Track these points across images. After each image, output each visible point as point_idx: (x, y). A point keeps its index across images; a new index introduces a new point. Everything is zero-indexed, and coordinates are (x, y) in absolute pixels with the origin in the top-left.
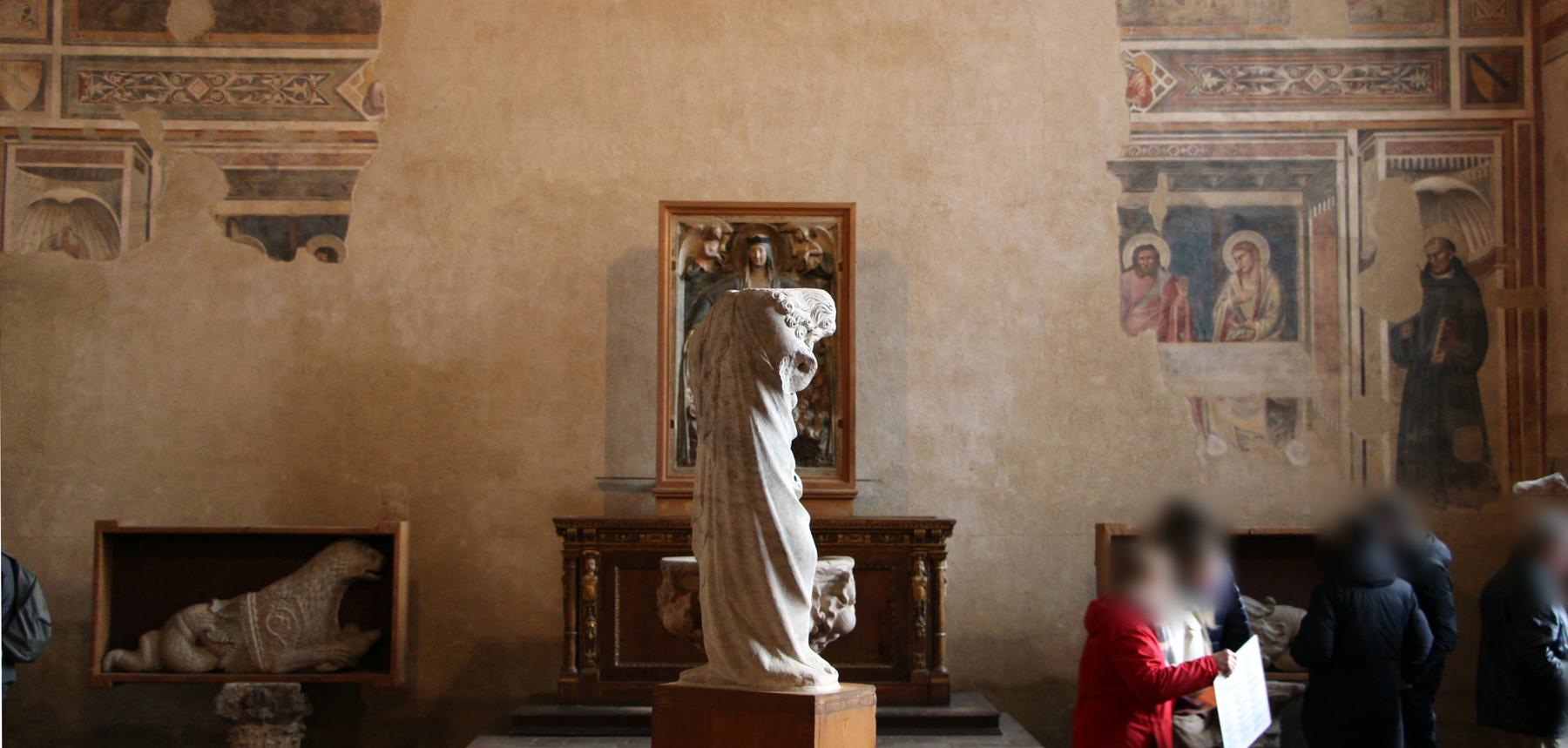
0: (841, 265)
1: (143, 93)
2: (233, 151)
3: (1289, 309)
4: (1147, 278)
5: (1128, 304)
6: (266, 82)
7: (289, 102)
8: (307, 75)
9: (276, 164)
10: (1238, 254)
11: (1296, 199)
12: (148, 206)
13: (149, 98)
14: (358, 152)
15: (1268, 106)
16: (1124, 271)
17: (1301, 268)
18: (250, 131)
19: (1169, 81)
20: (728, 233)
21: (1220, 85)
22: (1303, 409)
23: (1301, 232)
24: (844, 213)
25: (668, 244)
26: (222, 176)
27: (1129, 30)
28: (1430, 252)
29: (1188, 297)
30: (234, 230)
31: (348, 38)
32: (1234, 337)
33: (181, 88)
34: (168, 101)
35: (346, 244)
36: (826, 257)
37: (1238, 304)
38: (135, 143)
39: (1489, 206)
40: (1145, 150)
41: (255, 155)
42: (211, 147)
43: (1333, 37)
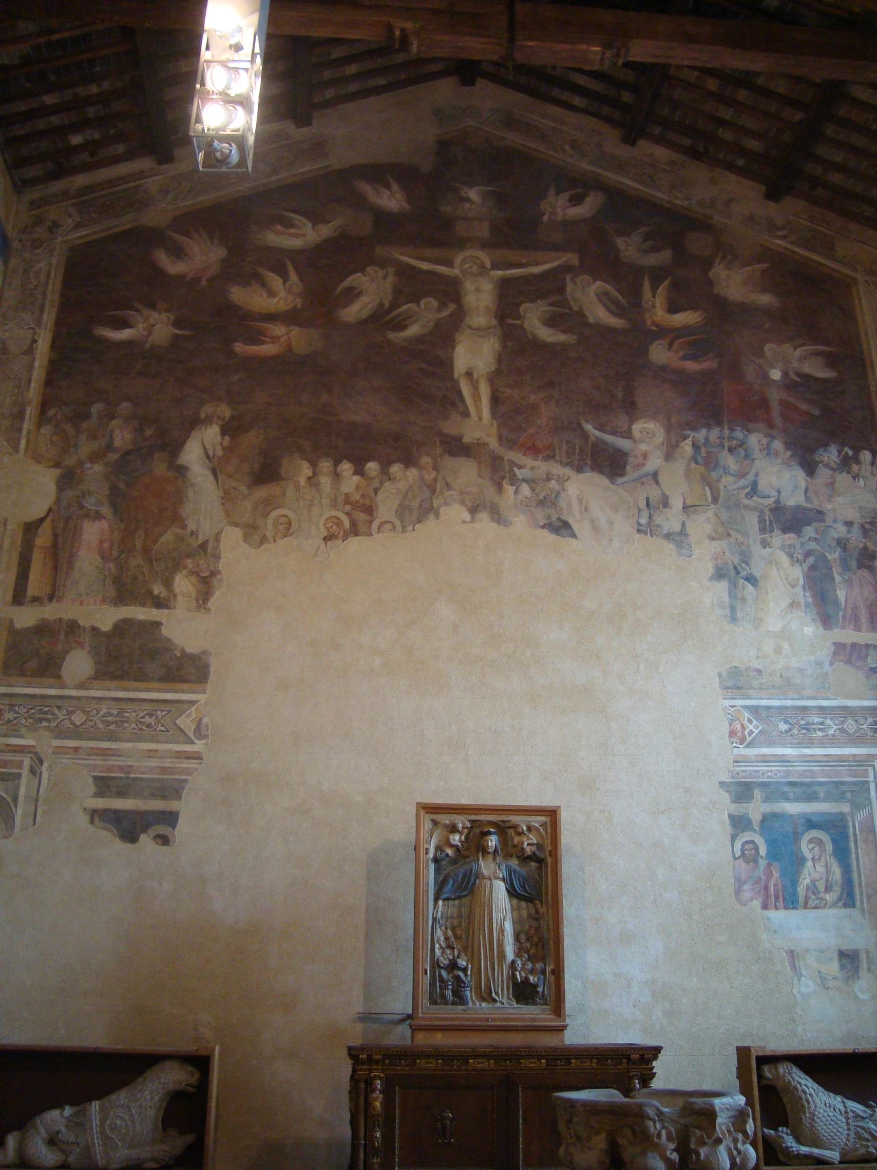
0: (550, 852)
1: (41, 720)
2: (99, 762)
3: (848, 884)
4: (752, 864)
5: (739, 883)
6: (126, 714)
7: (141, 729)
8: (156, 711)
9: (130, 773)
10: (811, 846)
11: (846, 808)
12: (37, 800)
13: (44, 724)
14: (188, 766)
15: (822, 745)
16: (735, 859)
17: (853, 856)
18: (113, 749)
19: (756, 727)
20: (466, 828)
21: (790, 730)
22: (863, 957)
23: (851, 831)
24: (552, 814)
25: (424, 834)
26: (90, 781)
27: (728, 692)
30: (96, 819)
31: (186, 686)
32: (813, 905)
33: (67, 717)
34: (57, 726)
35: (176, 832)
36: (539, 846)
37: (813, 882)
38: (32, 755)
40: (744, 774)
41: (114, 766)
42: (85, 759)
43: (858, 699)
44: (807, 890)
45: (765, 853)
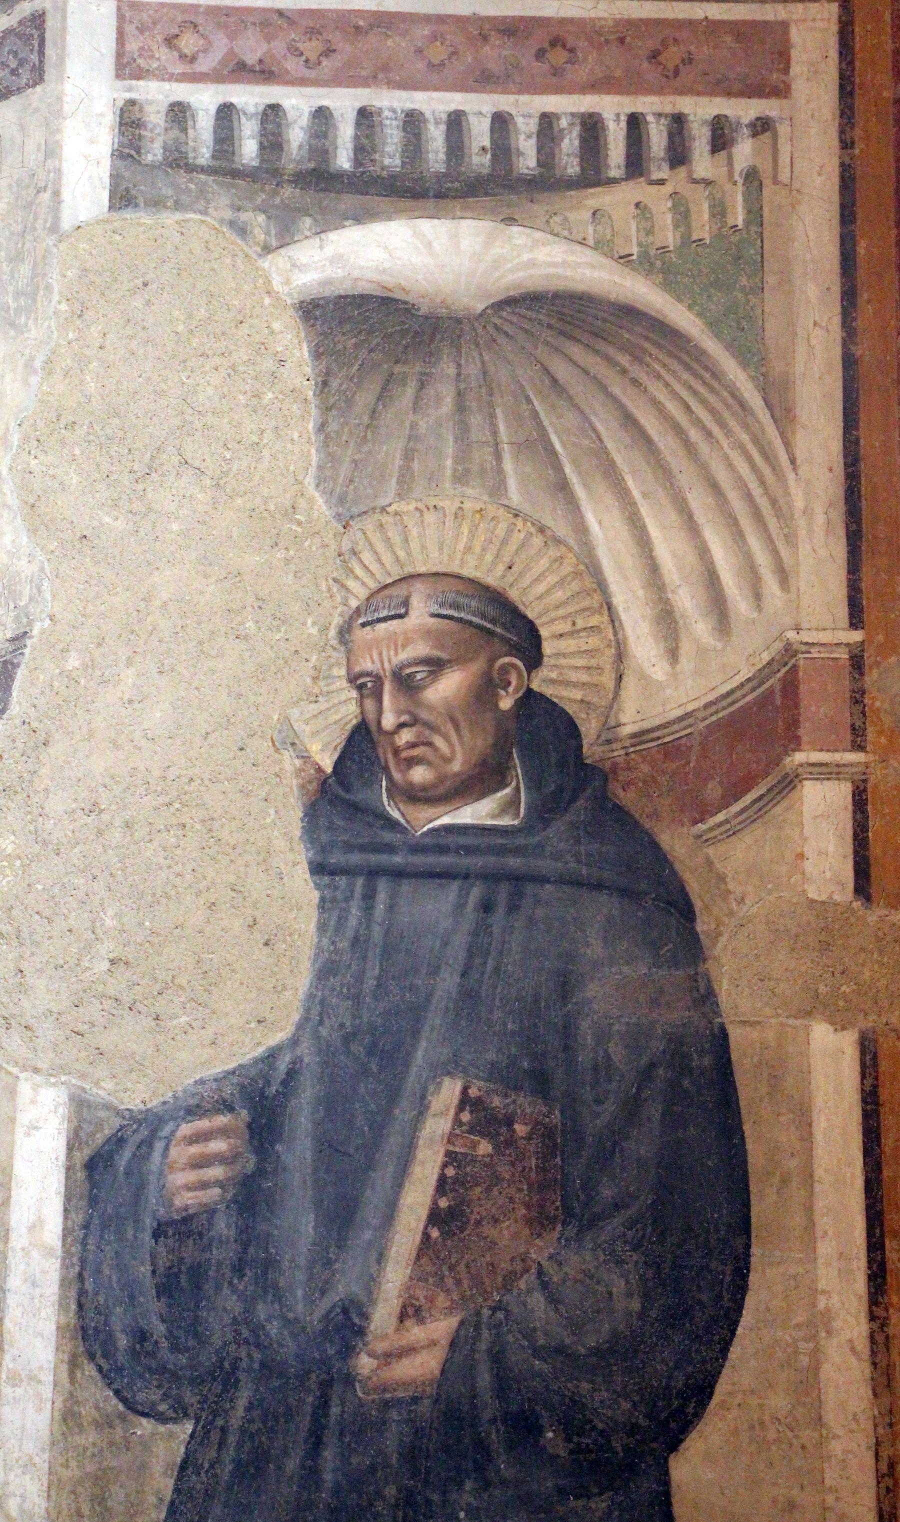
28: (366, 664)
39: (755, 401)
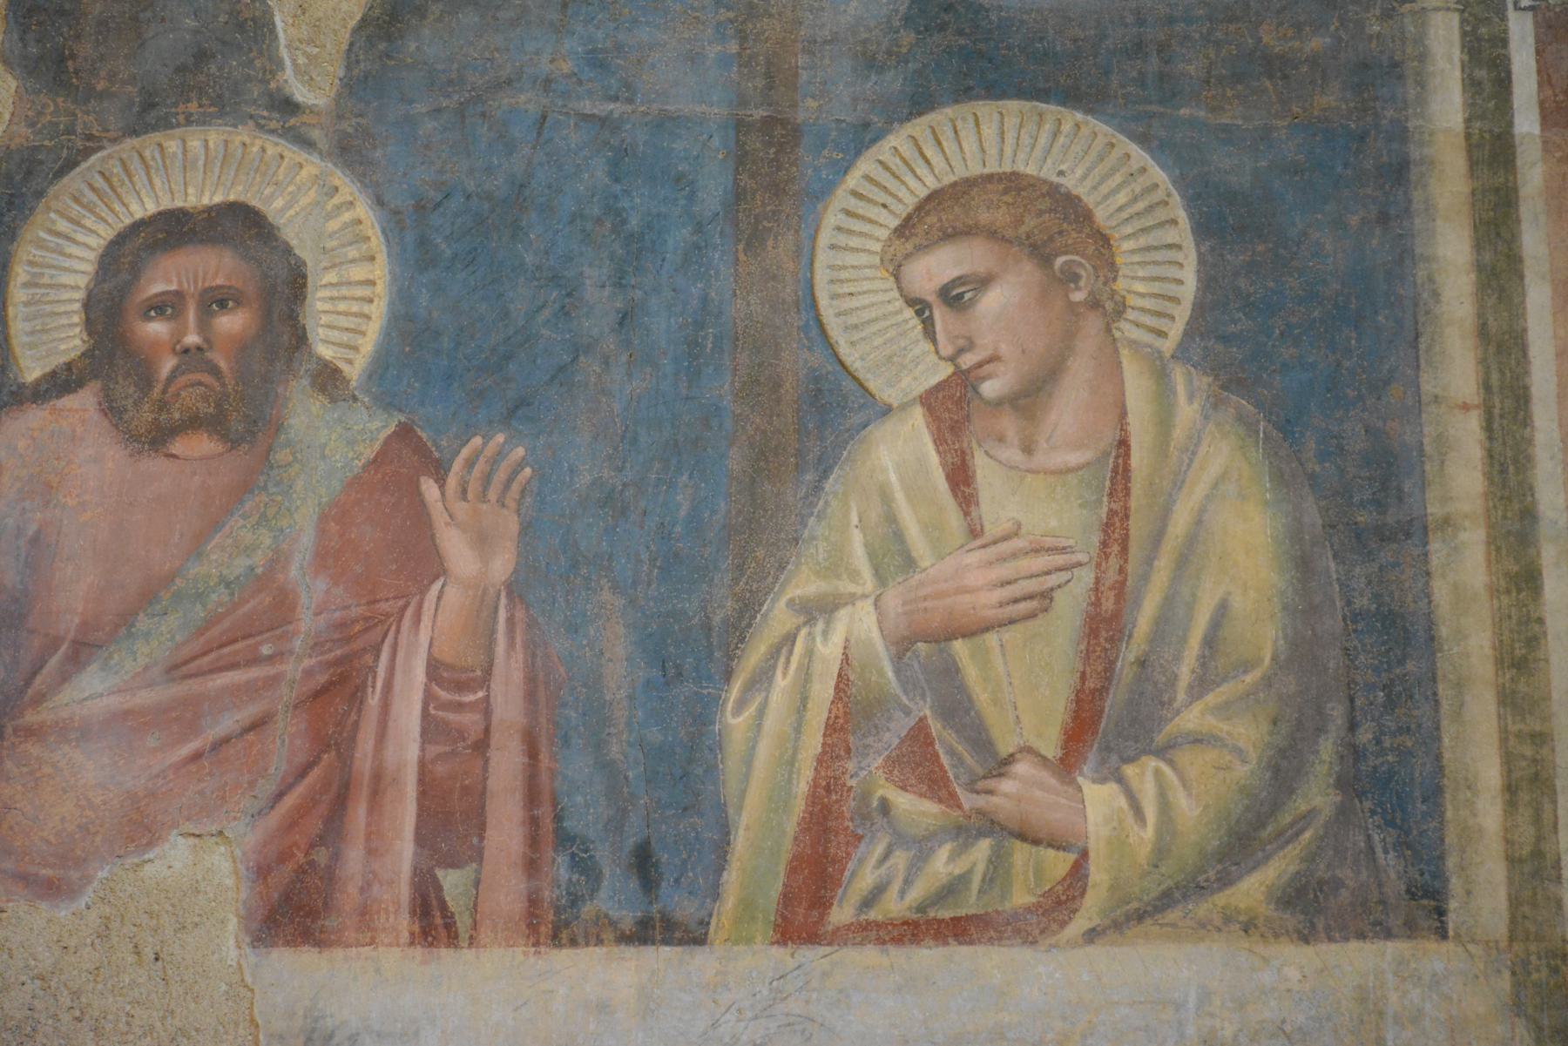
29: (514, 590)
32: (894, 906)
44: (831, 728)
45: (368, 344)
